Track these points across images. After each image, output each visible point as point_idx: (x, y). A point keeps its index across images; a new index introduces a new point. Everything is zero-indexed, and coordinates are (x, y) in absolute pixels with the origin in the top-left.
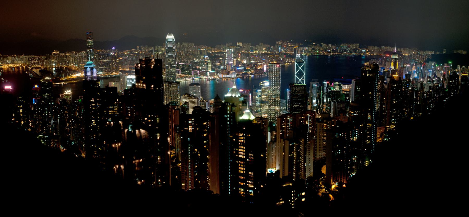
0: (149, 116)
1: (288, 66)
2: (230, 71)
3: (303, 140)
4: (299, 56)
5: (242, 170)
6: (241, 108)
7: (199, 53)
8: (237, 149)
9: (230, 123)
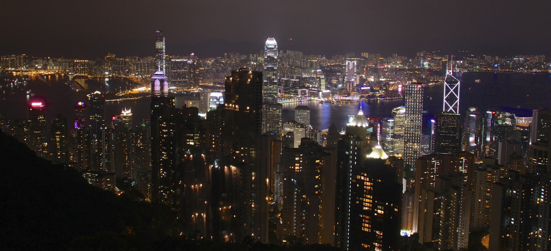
0: (242, 148)
1: (433, 86)
2: (351, 91)
3: (455, 194)
4: (450, 73)
5: (366, 228)
6: (369, 142)
7: (308, 65)
8: (361, 199)
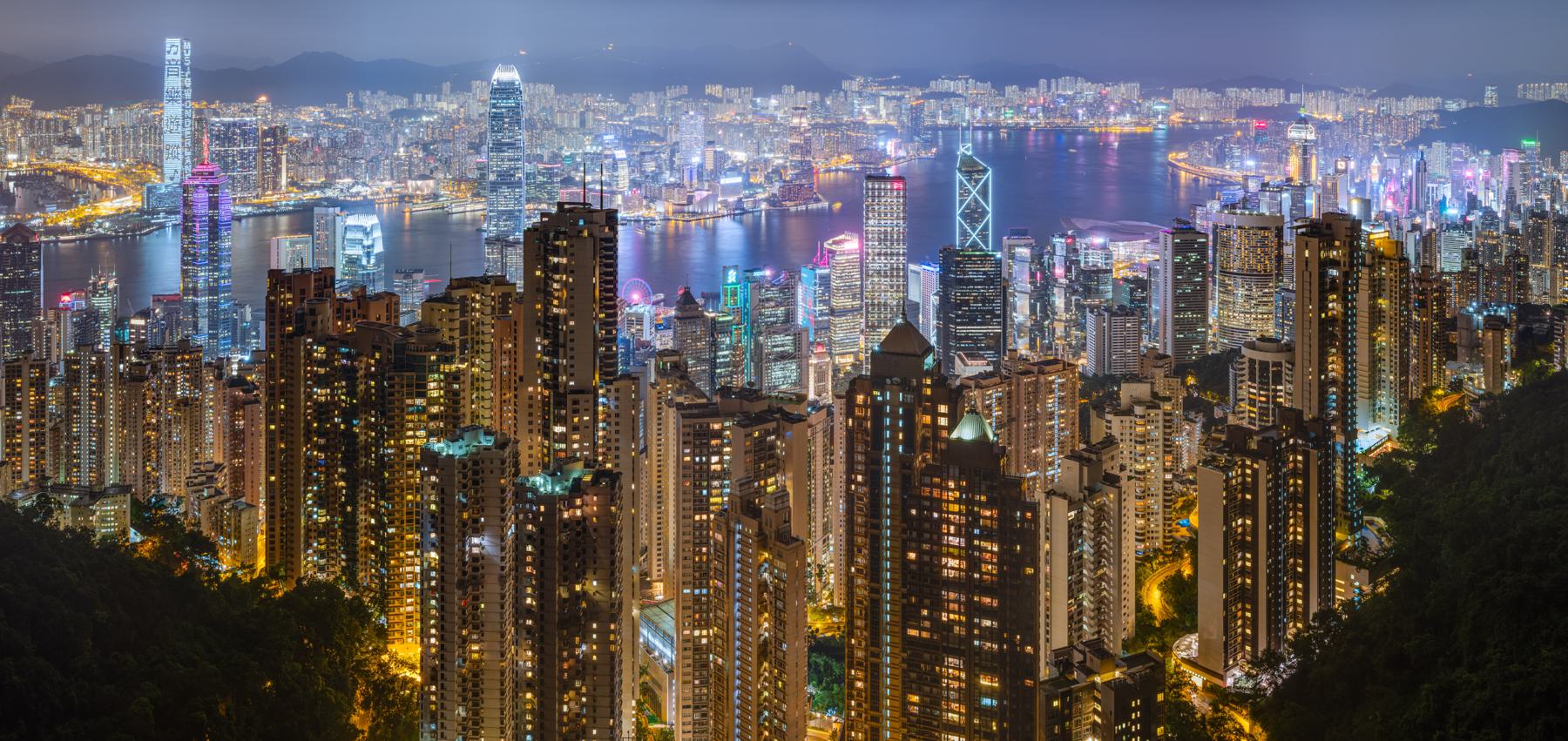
9: (893, 451)
